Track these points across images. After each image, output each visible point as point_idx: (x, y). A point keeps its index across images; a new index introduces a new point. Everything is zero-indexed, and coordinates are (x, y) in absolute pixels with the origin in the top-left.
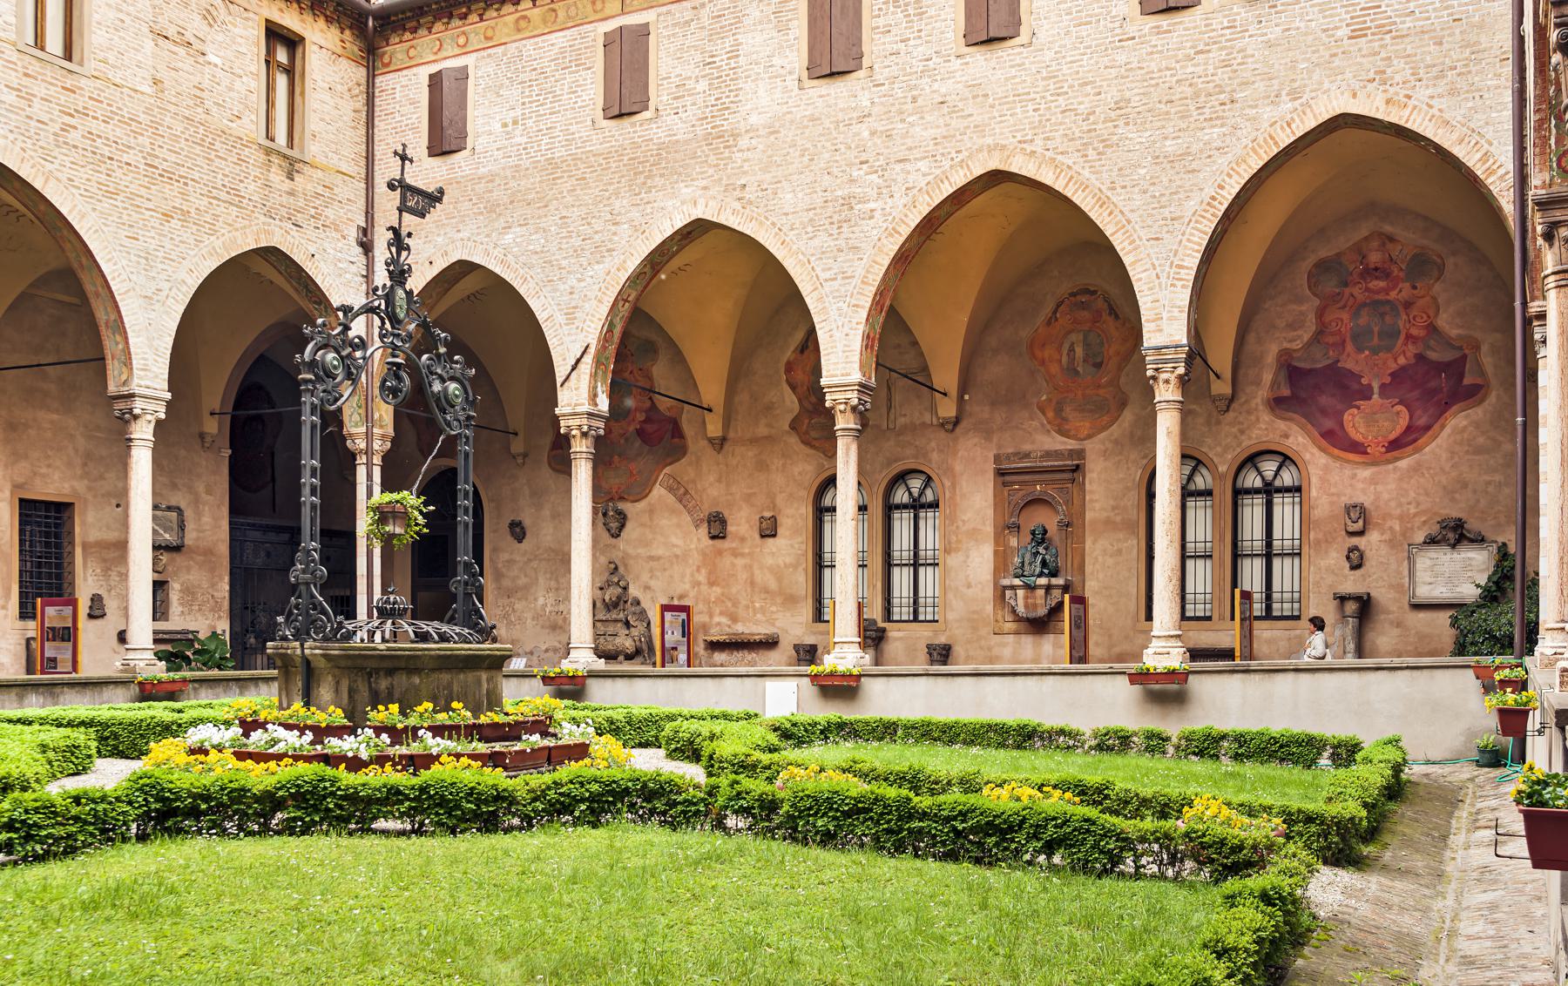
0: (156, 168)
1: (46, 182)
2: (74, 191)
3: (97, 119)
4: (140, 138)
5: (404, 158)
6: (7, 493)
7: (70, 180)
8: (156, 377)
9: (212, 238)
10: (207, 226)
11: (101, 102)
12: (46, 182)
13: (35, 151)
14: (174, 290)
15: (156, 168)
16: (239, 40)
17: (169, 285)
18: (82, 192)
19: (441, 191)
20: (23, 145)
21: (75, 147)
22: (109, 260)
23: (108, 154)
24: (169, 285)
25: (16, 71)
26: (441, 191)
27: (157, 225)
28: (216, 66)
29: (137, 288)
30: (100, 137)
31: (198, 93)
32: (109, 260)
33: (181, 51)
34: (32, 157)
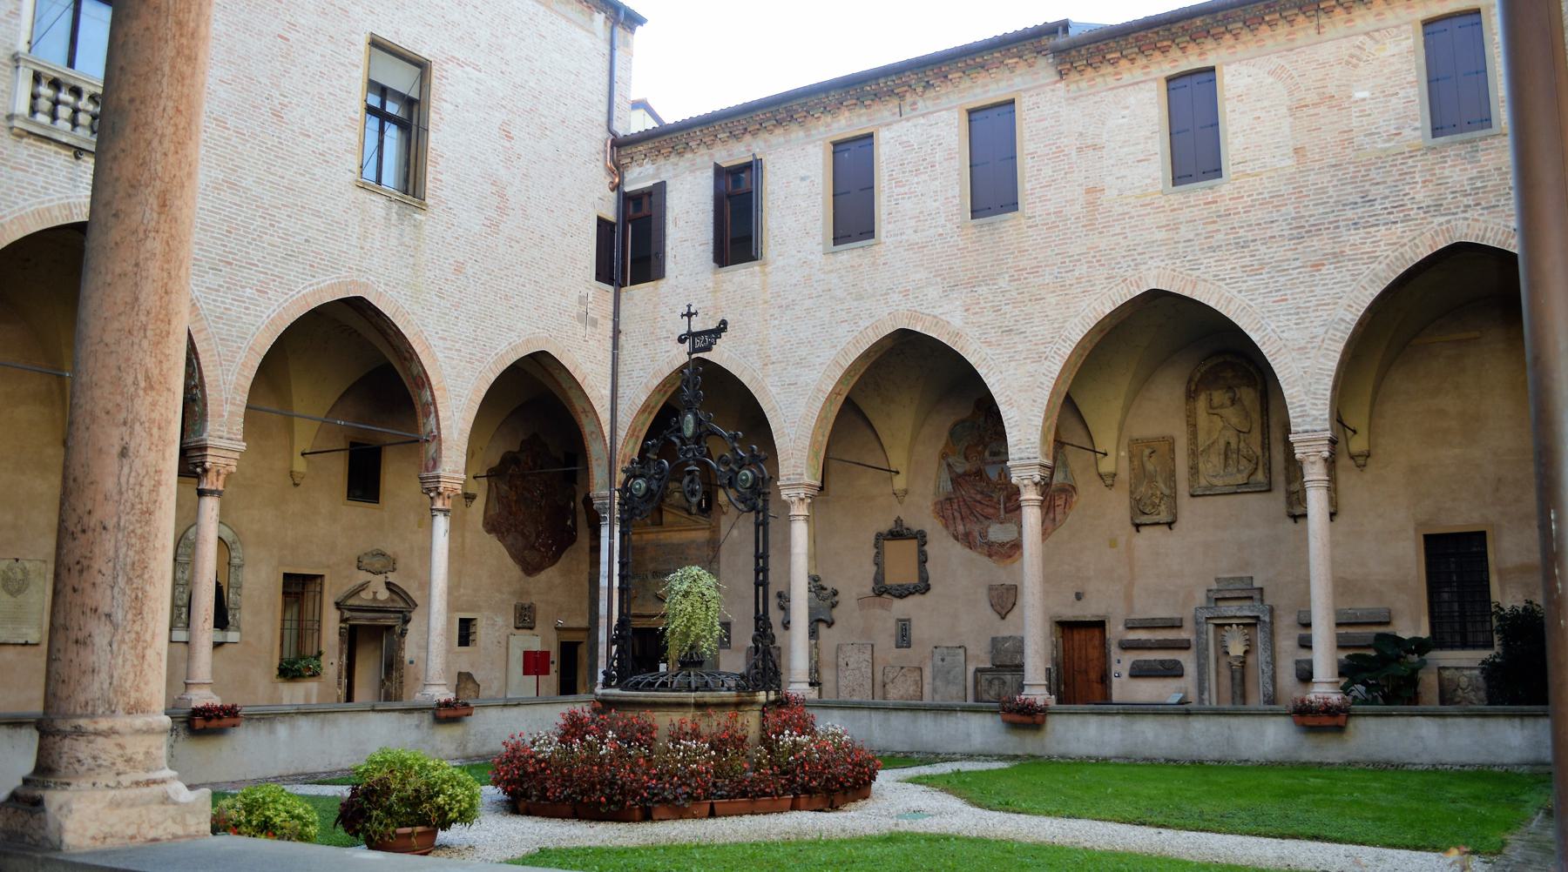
0: (1303, 227)
1: (1194, 287)
2: (1220, 283)
3: (1239, 213)
4: (1283, 209)
5: (689, 315)
6: (1411, 533)
7: (1215, 276)
8: (1316, 419)
9: (1372, 266)
10: (1365, 256)
11: (1242, 197)
12: (1194, 287)
13: (1184, 266)
14: (1331, 331)
15: (1303, 227)
16: (1391, 60)
17: (1324, 329)
18: (1228, 281)
19: (724, 322)
20: (1173, 267)
21: (1220, 246)
22: (1258, 329)
23: (1250, 238)
24: (1324, 329)
25: (1164, 211)
26: (724, 322)
27: (1307, 279)
28: (1364, 100)
29: (1290, 344)
30: (1242, 227)
31: (1346, 136)
32: (1258, 329)
33: (1323, 109)
34: (1181, 273)
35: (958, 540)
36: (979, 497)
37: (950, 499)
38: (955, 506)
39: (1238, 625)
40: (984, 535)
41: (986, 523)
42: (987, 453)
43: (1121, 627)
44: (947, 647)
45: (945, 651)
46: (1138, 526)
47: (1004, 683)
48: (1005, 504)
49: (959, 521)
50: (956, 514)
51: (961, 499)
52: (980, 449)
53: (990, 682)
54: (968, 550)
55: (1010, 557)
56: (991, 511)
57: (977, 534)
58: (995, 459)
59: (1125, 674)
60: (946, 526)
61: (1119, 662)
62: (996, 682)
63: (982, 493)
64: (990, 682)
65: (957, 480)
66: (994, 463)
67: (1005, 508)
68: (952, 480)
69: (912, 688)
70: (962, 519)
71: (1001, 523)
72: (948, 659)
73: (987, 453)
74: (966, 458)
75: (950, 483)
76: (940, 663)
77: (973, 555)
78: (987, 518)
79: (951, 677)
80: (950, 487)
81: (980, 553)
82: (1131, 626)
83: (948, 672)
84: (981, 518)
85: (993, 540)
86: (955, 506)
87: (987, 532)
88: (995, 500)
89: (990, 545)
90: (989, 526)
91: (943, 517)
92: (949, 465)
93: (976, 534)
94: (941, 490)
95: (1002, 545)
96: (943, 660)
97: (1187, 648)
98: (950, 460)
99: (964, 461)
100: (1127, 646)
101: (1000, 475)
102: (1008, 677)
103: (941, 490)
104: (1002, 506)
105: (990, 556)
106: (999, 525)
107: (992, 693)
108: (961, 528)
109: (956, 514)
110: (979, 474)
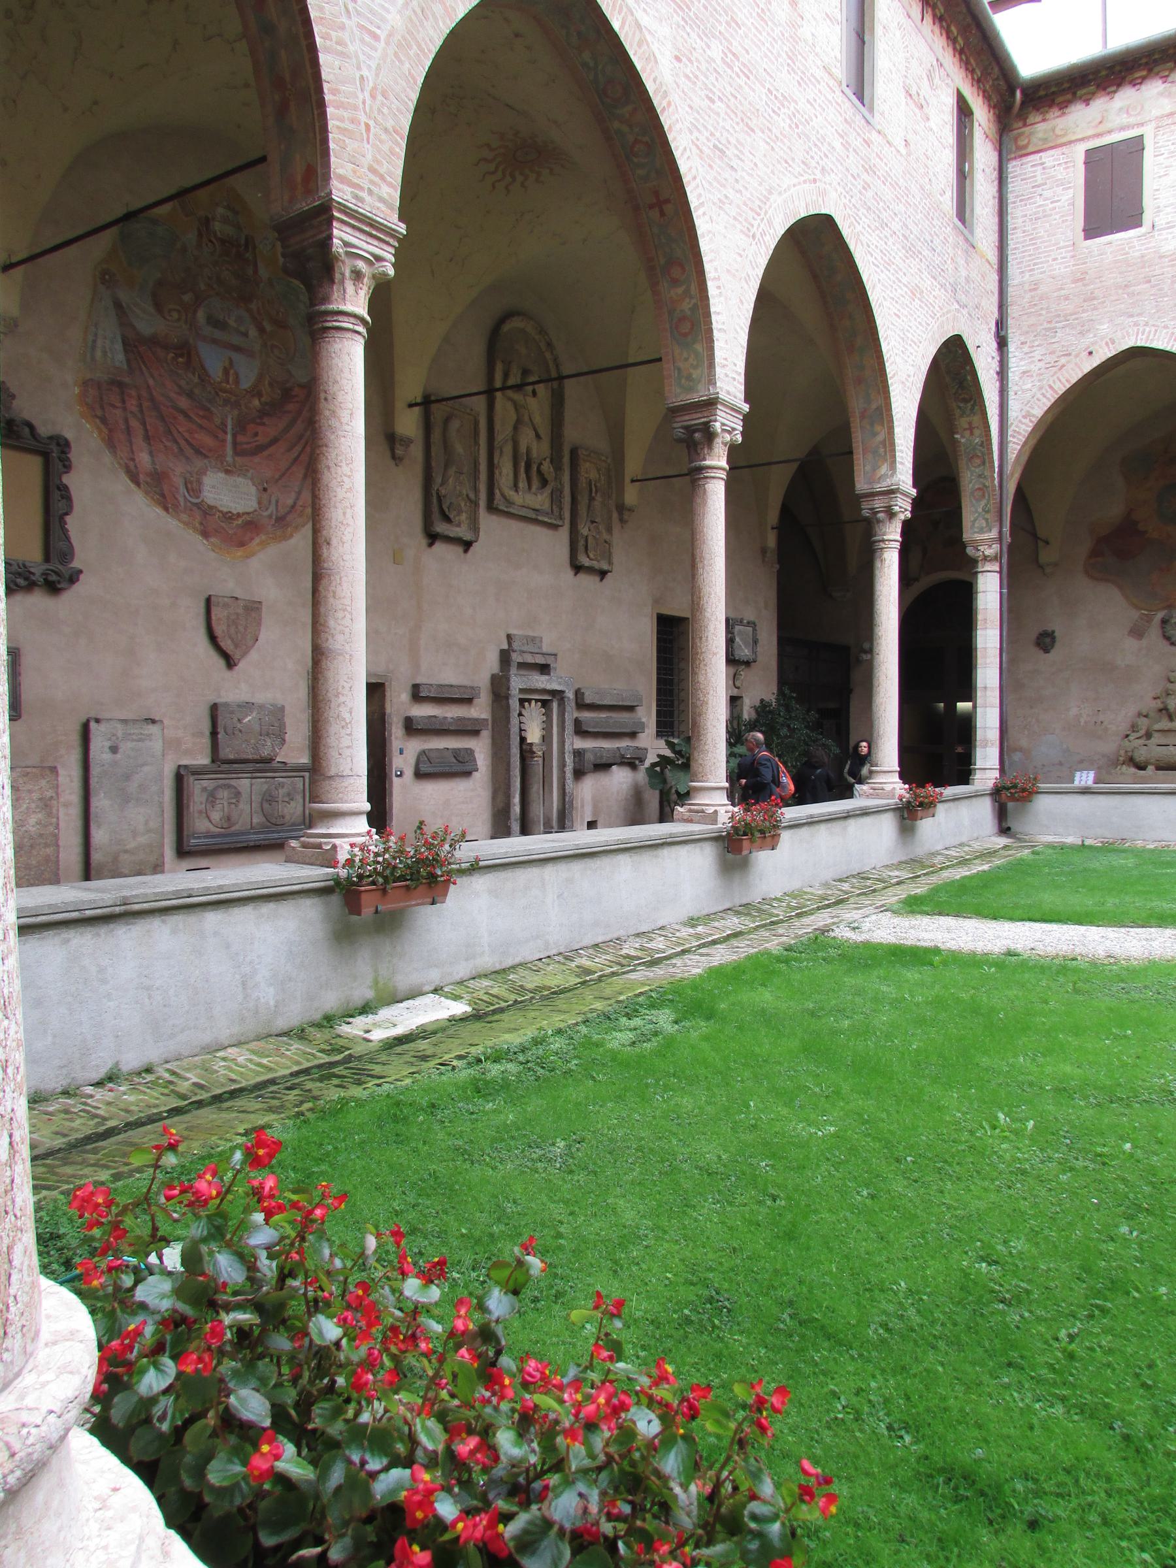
35: (138, 484)
36: (183, 403)
37: (121, 385)
38: (132, 404)
39: (537, 701)
40: (194, 488)
41: (199, 463)
42: (201, 315)
43: (405, 697)
44: (125, 722)
45: (120, 730)
46: (432, 538)
47: (238, 794)
48: (234, 436)
49: (139, 441)
50: (134, 423)
51: (144, 394)
52: (187, 298)
53: (212, 797)
54: (159, 511)
55: (242, 544)
56: (208, 441)
57: (179, 482)
58: (218, 334)
59: (409, 772)
60: (111, 444)
61: (401, 752)
62: (224, 794)
63: (190, 395)
64: (212, 797)
65: (133, 345)
66: (215, 341)
67: (235, 443)
68: (126, 343)
69: (33, 820)
70: (147, 438)
71: (227, 472)
72: (126, 747)
73: (201, 315)
74: (158, 307)
75: (119, 346)
76: (107, 756)
77: (171, 523)
78: (198, 452)
79: (133, 787)
80: (120, 357)
81: (186, 524)
82: (417, 694)
83: (128, 777)
84: (189, 451)
85: (211, 502)
86: (132, 404)
87: (200, 483)
88: (218, 421)
89: (207, 511)
90: (203, 472)
91: (104, 420)
92: (118, 305)
93: (179, 482)
94: (99, 354)
95: (229, 517)
96: (114, 749)
97: (475, 733)
98: (123, 296)
99: (151, 310)
100: (411, 727)
101: (226, 372)
102: (244, 784)
103: (99, 354)
104: (229, 437)
105: (205, 534)
106: (222, 475)
107: (216, 816)
108: (144, 458)
109: (134, 423)
110: (185, 352)
